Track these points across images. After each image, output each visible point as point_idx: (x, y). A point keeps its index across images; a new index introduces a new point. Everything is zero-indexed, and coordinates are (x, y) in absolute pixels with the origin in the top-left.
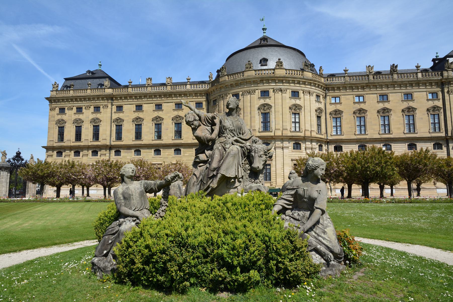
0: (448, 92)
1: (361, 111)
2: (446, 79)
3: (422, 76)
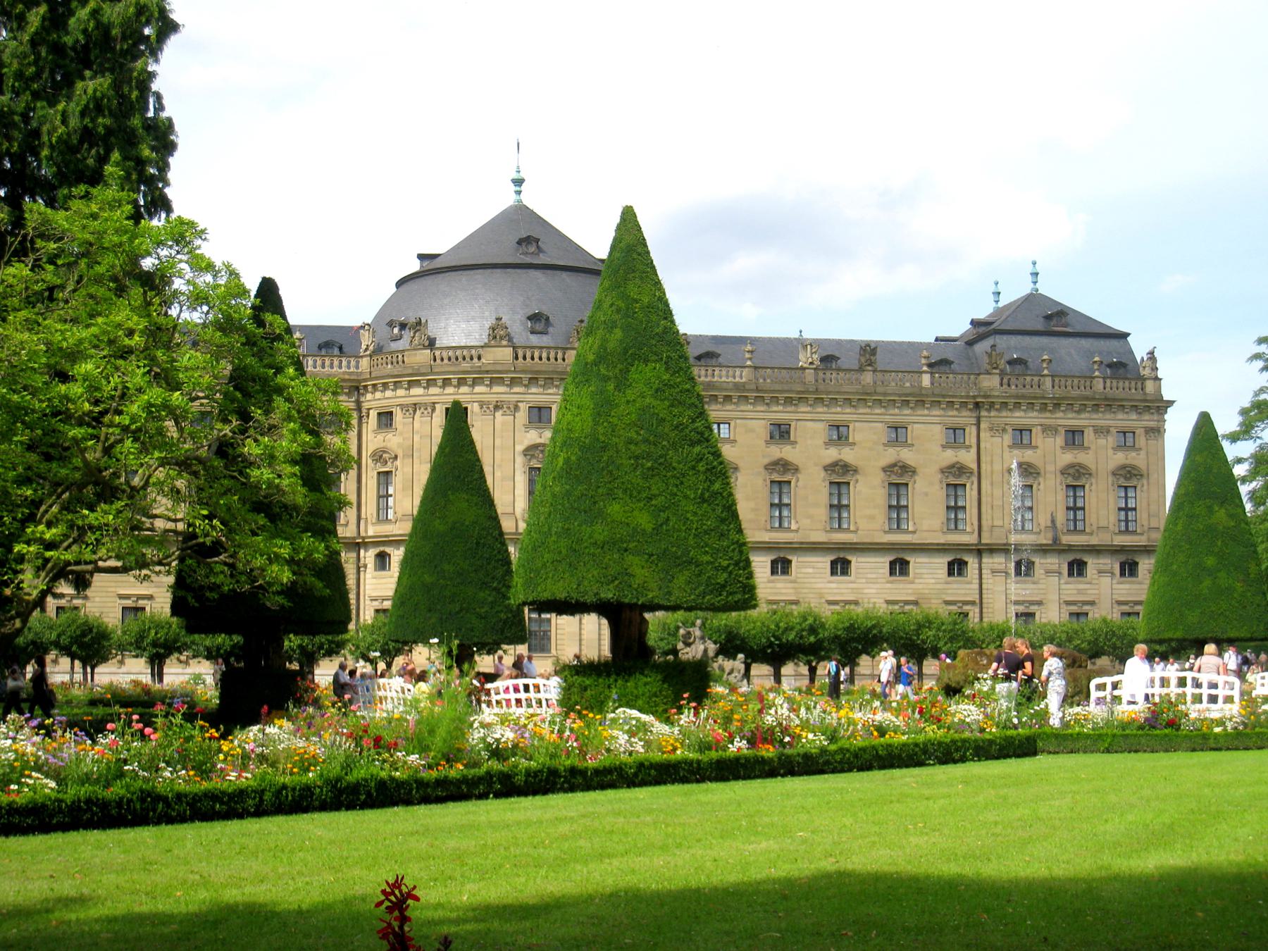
0: (991, 429)
1: (783, 466)
2: (985, 396)
3: (932, 384)
